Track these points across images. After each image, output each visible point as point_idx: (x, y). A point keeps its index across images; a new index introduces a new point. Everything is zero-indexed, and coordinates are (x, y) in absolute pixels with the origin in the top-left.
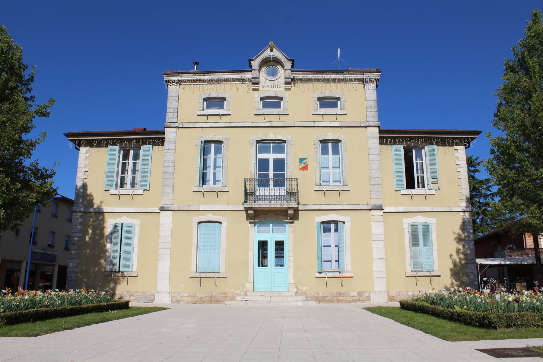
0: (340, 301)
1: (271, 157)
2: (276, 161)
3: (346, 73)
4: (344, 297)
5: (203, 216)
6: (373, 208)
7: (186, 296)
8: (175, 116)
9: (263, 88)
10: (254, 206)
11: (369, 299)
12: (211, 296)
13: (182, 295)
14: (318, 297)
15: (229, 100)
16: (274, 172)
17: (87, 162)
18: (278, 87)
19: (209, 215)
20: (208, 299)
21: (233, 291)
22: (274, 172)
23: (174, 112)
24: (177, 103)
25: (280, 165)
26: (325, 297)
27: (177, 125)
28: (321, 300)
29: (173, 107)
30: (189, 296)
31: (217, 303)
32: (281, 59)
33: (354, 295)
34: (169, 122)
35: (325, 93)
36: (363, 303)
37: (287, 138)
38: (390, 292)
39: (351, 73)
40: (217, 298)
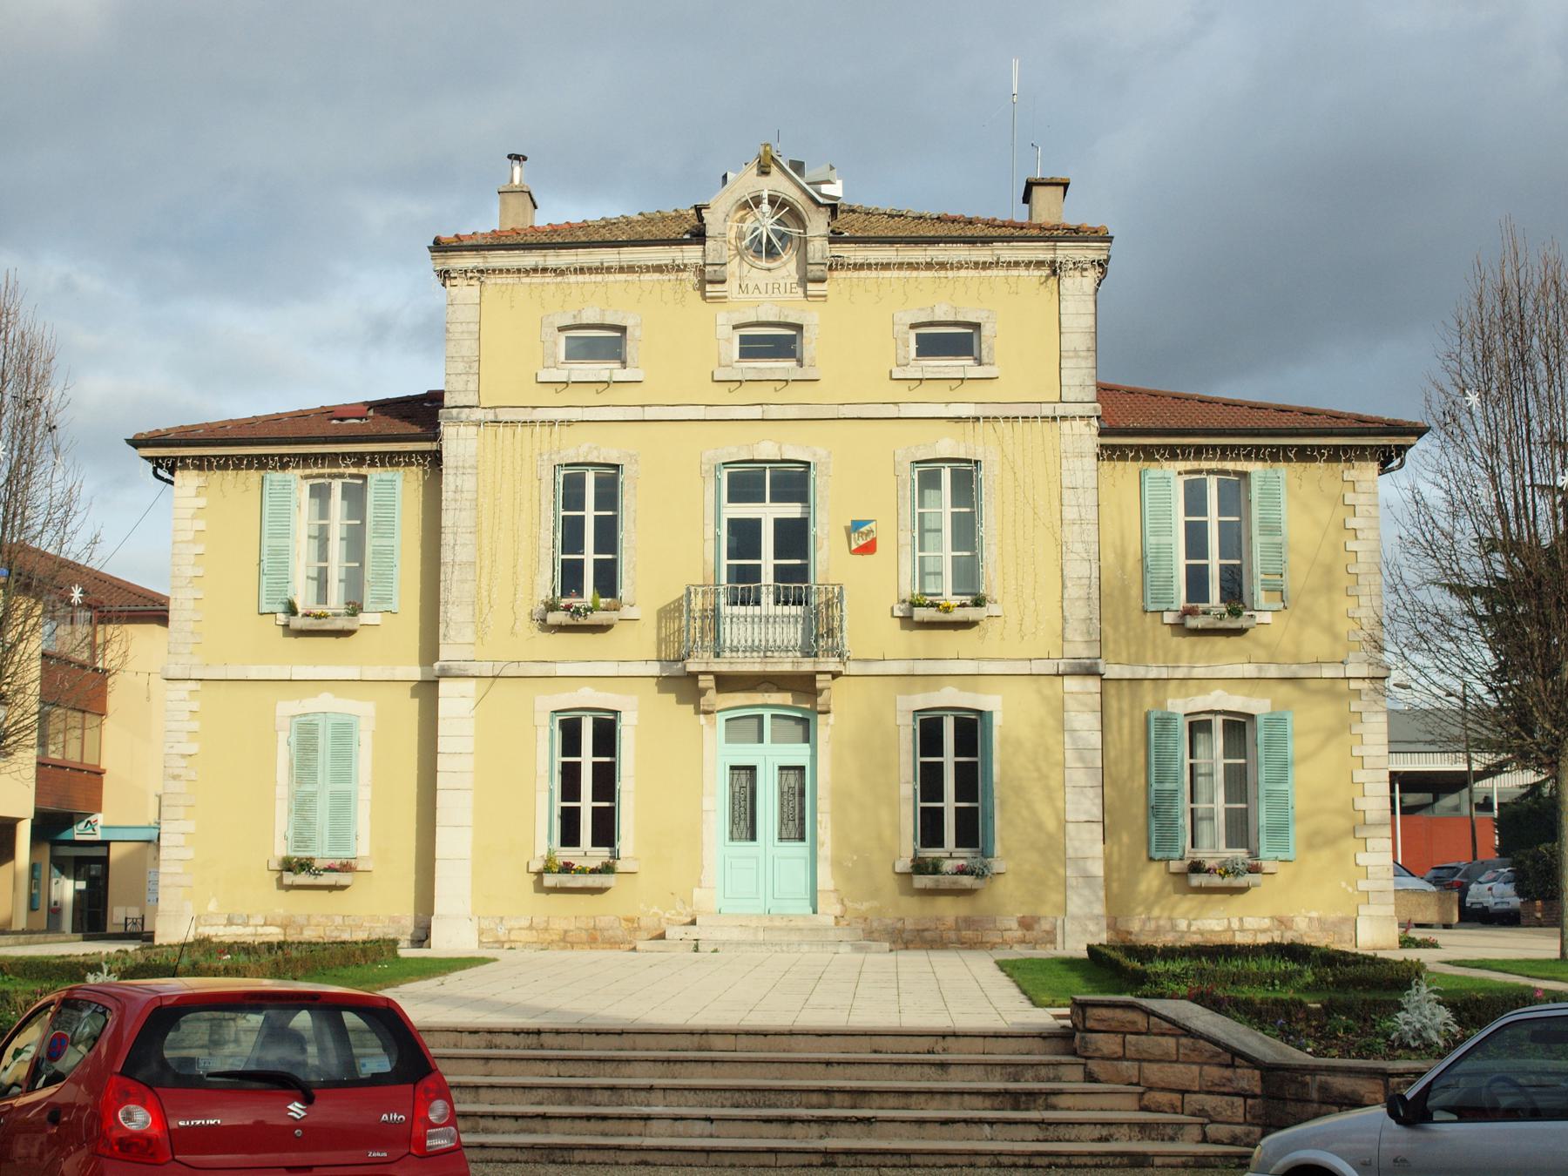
0: (965, 943)
1: (768, 513)
2: (780, 524)
3: (1000, 244)
4: (977, 930)
5: (567, 694)
6: (1069, 670)
7: (520, 929)
8: (473, 386)
9: (741, 295)
10: (716, 668)
11: (1050, 937)
12: (595, 928)
13: (508, 924)
14: (902, 931)
15: (637, 333)
16: (775, 558)
17: (201, 525)
18: (788, 290)
19: (582, 690)
20: (584, 935)
21: (656, 914)
22: (775, 558)
23: (467, 373)
24: (475, 346)
25: (793, 537)
26: (923, 930)
27: (478, 414)
28: (912, 941)
29: (463, 357)
30: (531, 928)
31: (611, 948)
32: (795, 203)
33: (1008, 927)
34: (453, 405)
35: (932, 309)
36: (1035, 949)
37: (815, 455)
38: (1119, 919)
39: (1015, 244)
40: (610, 932)
